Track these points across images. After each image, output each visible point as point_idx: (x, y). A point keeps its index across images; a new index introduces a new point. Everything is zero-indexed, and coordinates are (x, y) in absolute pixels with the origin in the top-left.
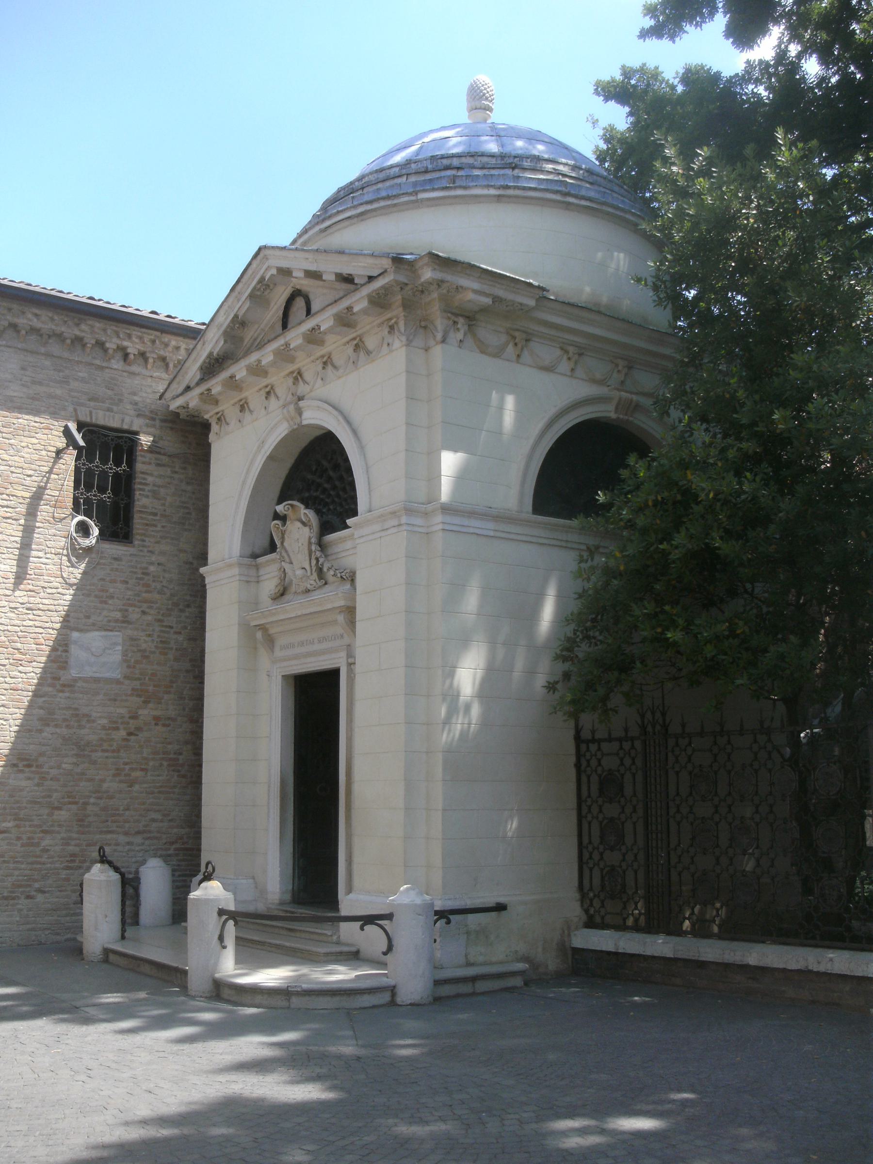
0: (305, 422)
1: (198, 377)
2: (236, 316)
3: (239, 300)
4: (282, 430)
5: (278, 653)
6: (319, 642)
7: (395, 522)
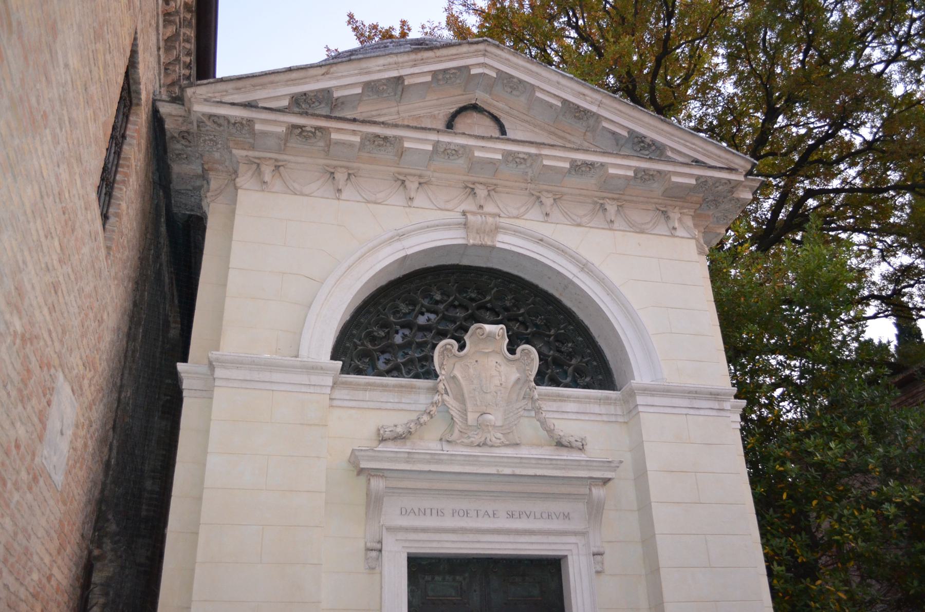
0: (499, 245)
1: (285, 103)
2: (399, 79)
3: (415, 65)
4: (452, 237)
5: (392, 515)
6: (511, 516)
7: (716, 405)
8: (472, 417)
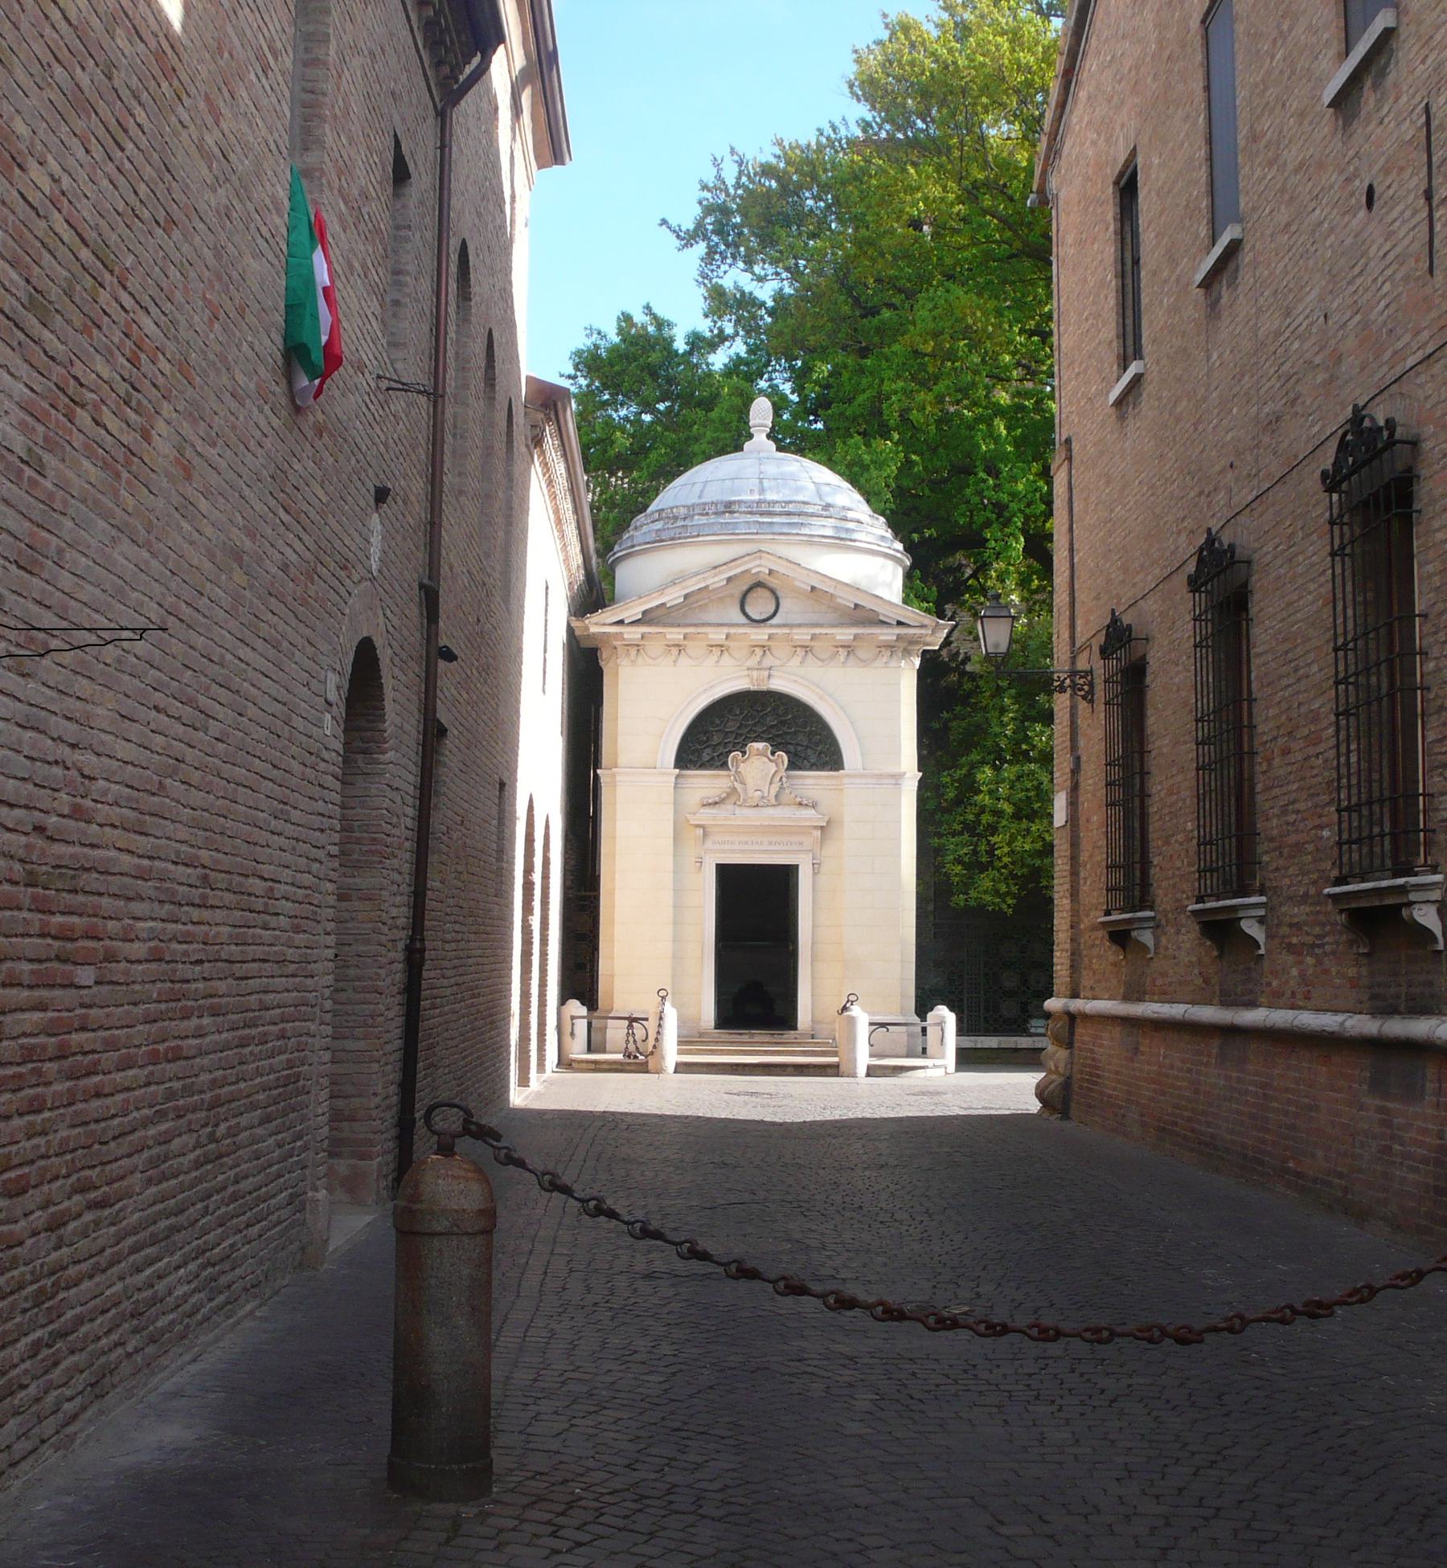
2: (706, 587)
5: (709, 844)
8: (750, 793)
